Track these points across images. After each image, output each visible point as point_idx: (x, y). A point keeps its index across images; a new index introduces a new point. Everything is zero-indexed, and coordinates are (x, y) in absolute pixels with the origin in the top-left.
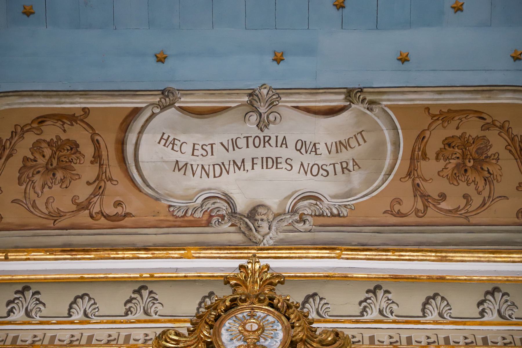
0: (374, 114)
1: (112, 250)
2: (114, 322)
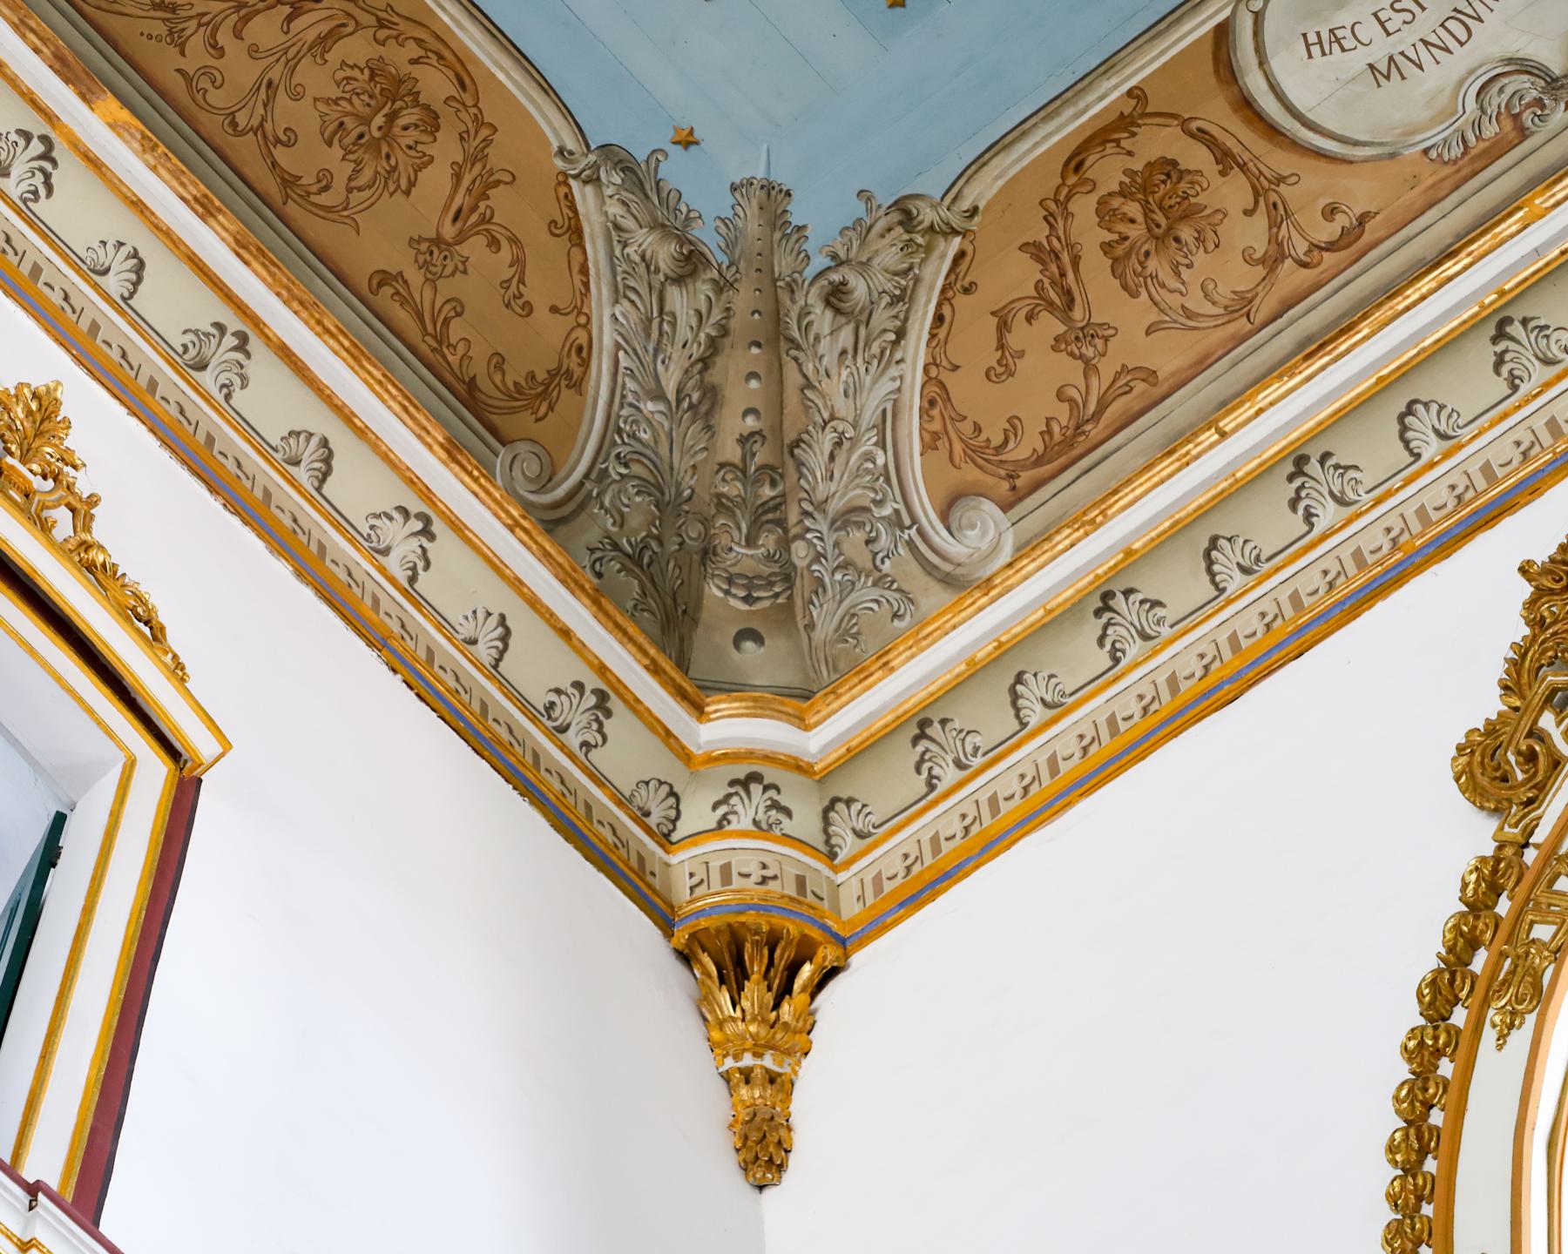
1: (1390, 298)
2: (1505, 416)
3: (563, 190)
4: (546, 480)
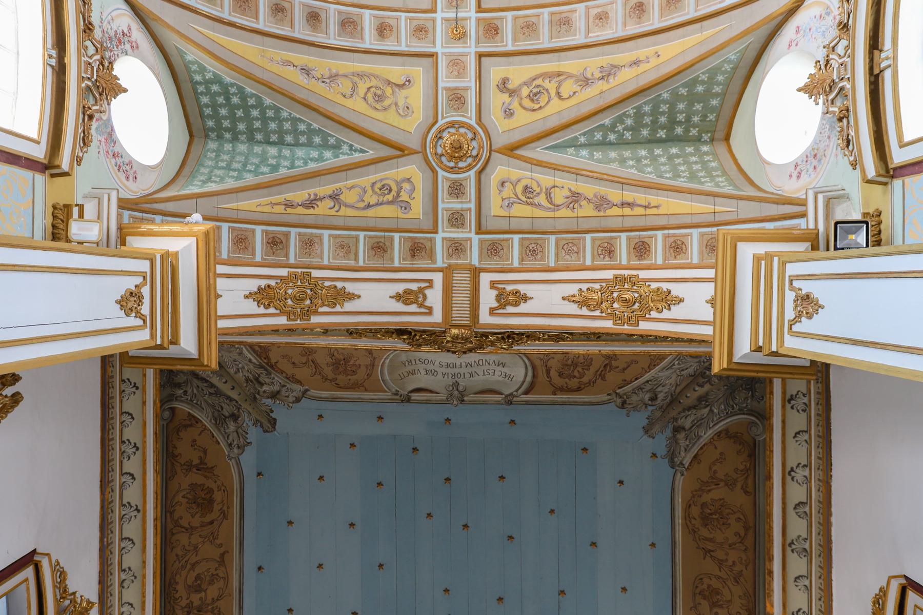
3: (689, 467)
4: (753, 423)
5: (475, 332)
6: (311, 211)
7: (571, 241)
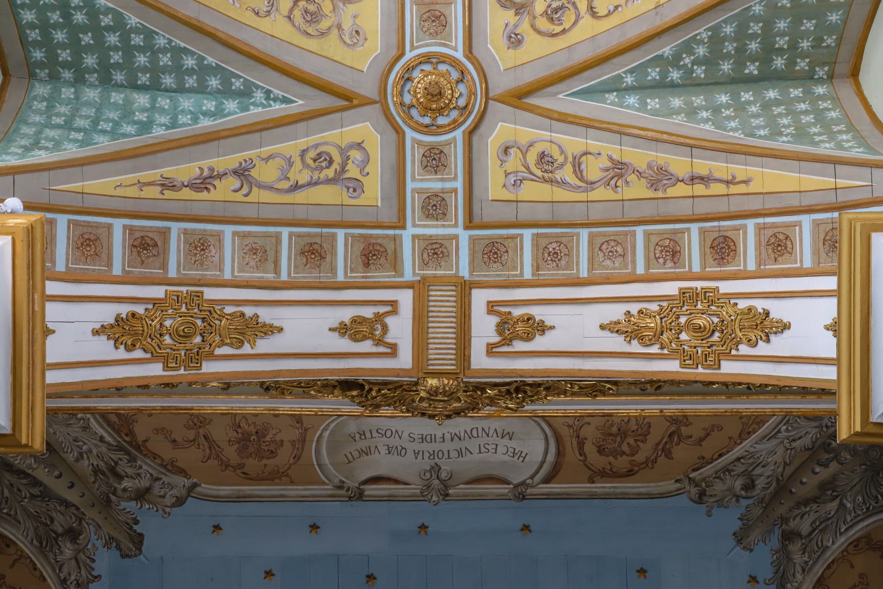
0: (338, 477)
5: (464, 382)
6: (204, 195)
7: (612, 238)
